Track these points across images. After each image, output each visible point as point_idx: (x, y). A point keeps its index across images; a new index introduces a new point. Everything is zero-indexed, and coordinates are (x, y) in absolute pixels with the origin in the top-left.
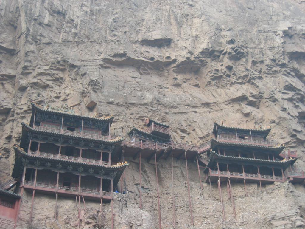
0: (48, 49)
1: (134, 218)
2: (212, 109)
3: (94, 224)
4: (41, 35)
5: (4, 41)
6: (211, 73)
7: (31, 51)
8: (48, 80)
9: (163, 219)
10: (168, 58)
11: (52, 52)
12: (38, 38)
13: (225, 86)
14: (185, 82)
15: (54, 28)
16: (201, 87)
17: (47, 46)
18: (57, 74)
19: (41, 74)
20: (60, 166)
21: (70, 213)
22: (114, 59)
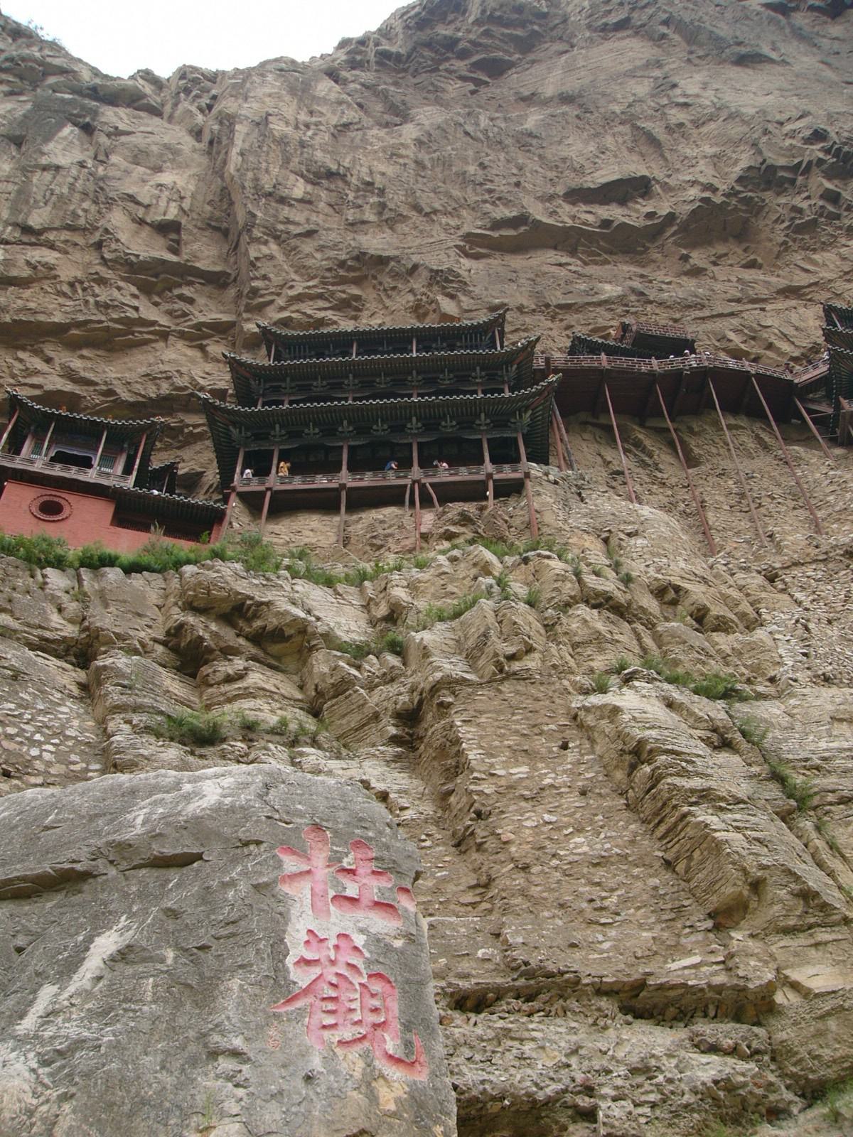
0: (308, 247)
1: (612, 517)
2: (810, 300)
3: (470, 535)
4: (288, 221)
5: (195, 257)
6: (783, 221)
7: (265, 256)
8: (319, 309)
9: (719, 531)
10: (650, 215)
11: (321, 249)
12: (281, 227)
13: (832, 243)
14: (715, 264)
15: (322, 205)
16: (765, 266)
17: (307, 240)
18: (344, 292)
19: (300, 298)
20: (346, 427)
21: (386, 526)
22: (496, 234)
